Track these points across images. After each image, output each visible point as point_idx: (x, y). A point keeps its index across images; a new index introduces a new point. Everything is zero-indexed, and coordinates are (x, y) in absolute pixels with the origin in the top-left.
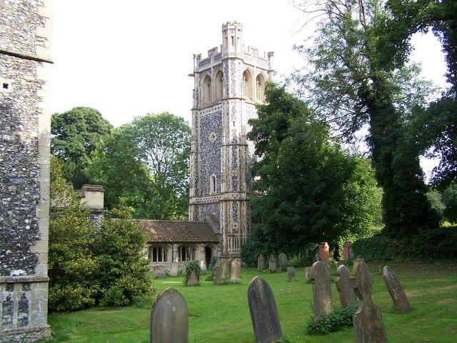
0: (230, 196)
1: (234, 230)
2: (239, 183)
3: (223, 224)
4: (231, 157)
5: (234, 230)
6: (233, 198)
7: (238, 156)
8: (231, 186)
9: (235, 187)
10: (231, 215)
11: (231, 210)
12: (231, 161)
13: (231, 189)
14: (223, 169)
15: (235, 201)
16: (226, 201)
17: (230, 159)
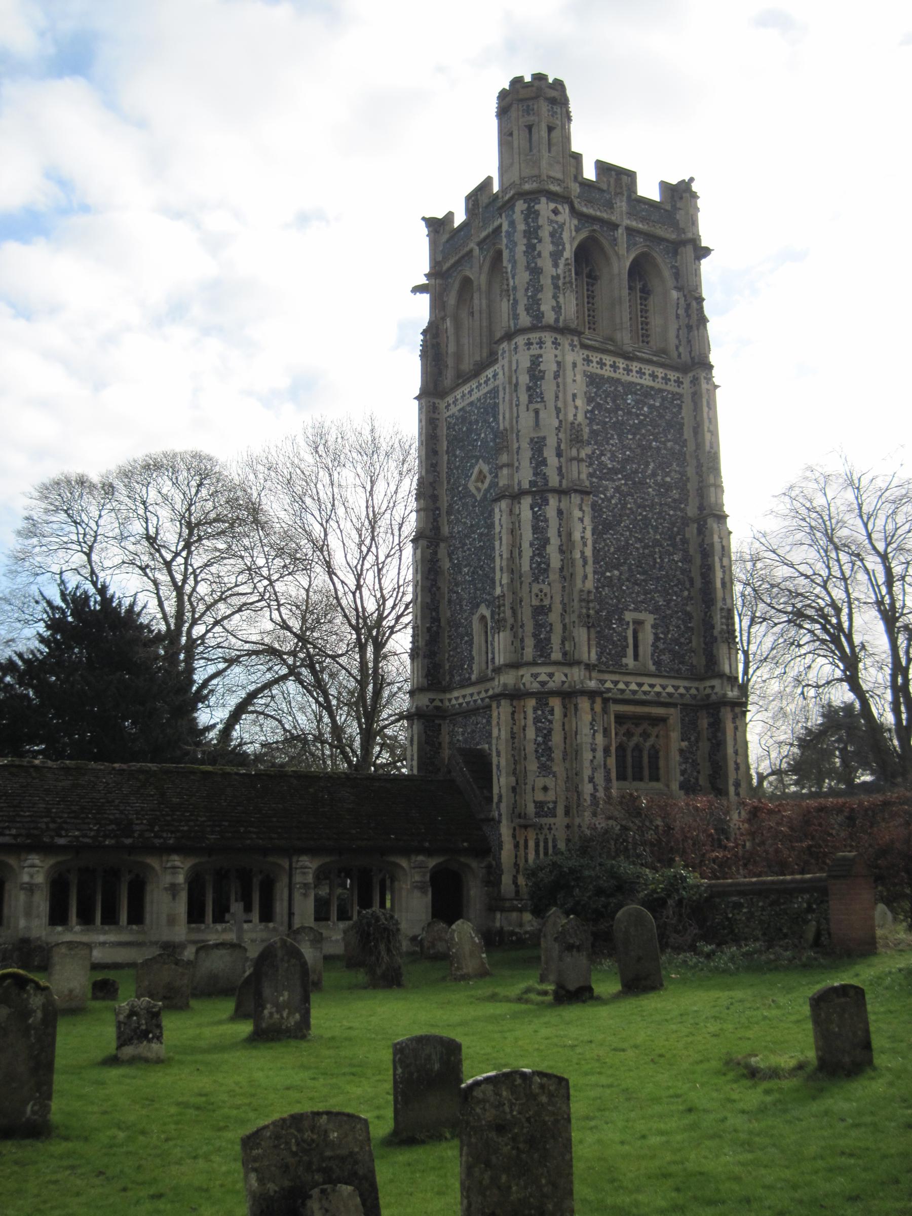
0: (527, 678)
1: (539, 805)
2: (558, 629)
3: (501, 782)
4: (527, 535)
5: (539, 805)
6: (535, 687)
7: (552, 533)
8: (530, 642)
9: (543, 647)
10: (530, 748)
11: (531, 733)
12: (527, 552)
13: (529, 653)
14: (502, 579)
15: (542, 697)
16: (515, 695)
17: (526, 545)
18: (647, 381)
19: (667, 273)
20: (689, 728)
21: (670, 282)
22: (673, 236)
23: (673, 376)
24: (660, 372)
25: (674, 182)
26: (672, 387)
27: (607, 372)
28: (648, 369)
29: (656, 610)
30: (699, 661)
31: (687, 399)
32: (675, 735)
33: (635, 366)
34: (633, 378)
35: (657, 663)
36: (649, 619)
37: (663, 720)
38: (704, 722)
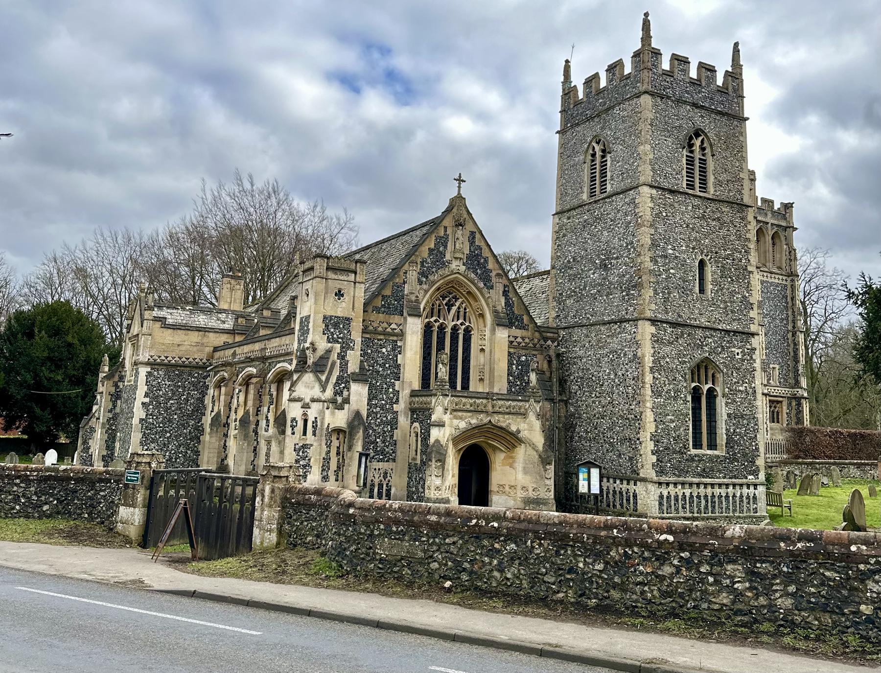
18: (777, 281)
19: (783, 238)
20: (790, 404)
21: (784, 242)
22: (784, 224)
23: (784, 278)
24: (781, 277)
25: (786, 202)
26: (784, 282)
27: (765, 279)
28: (777, 276)
29: (779, 364)
30: (792, 381)
31: (789, 287)
32: (785, 408)
33: (773, 276)
34: (773, 280)
35: (780, 382)
36: (777, 367)
37: (781, 402)
38: (794, 404)
